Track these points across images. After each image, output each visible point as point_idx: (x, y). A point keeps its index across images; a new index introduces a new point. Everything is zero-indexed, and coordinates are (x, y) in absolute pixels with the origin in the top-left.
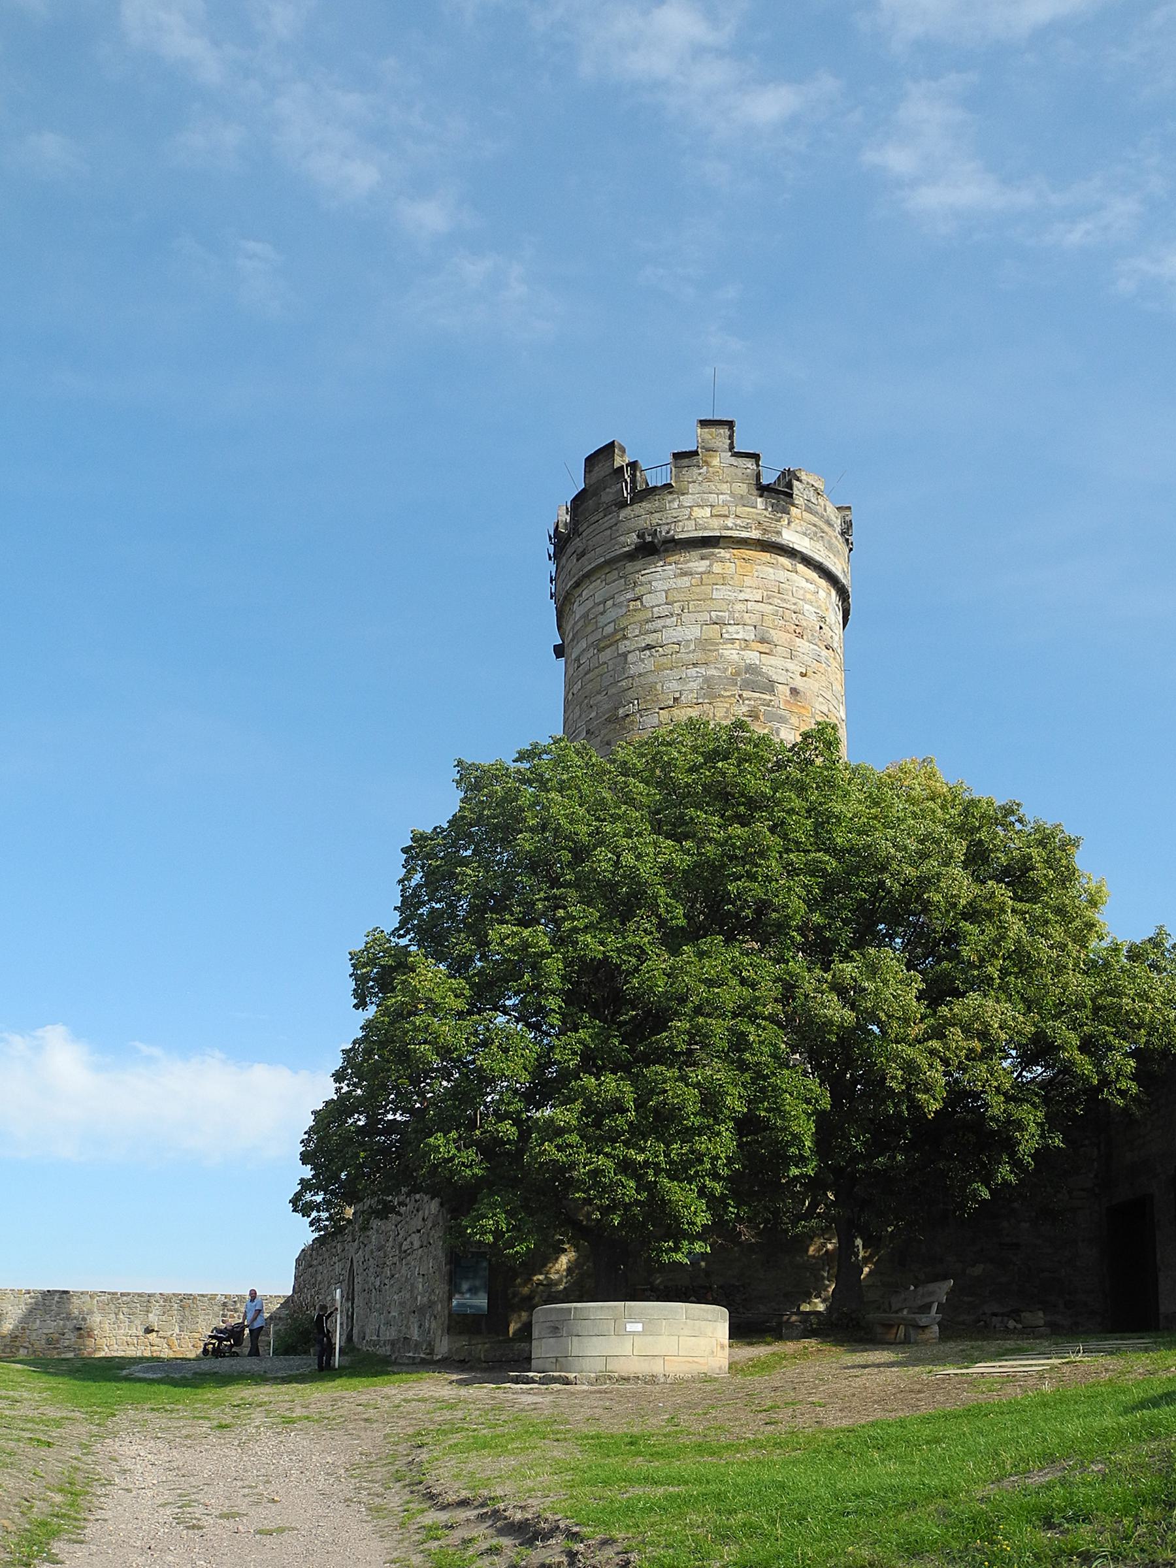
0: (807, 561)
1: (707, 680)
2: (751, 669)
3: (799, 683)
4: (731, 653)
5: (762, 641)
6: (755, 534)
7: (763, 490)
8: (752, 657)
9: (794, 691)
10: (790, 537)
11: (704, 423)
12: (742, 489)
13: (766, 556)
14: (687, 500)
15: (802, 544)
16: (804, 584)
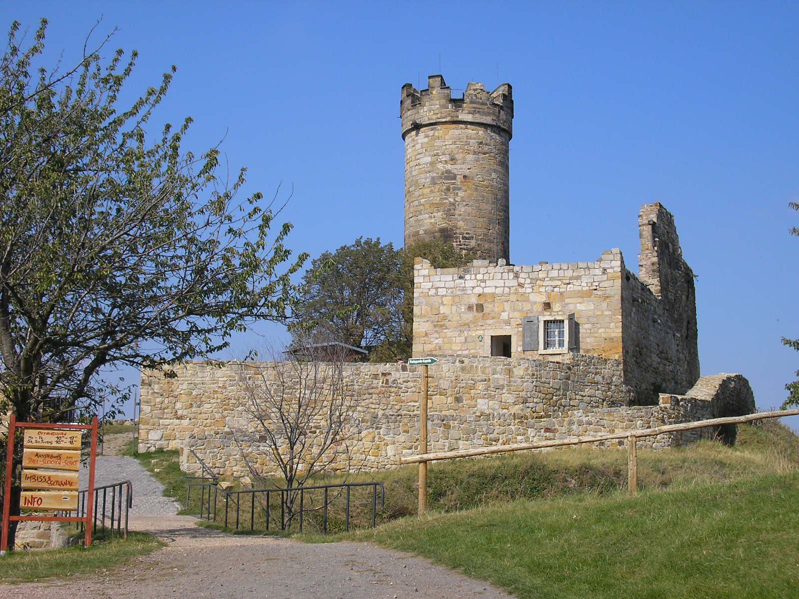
0: (472, 123)
1: (433, 178)
2: (448, 172)
3: (467, 172)
4: (440, 166)
5: (452, 160)
6: (448, 119)
7: (453, 101)
8: (449, 167)
9: (465, 177)
10: (464, 116)
11: (430, 77)
12: (443, 101)
13: (454, 126)
14: (425, 109)
15: (469, 118)
16: (470, 131)
